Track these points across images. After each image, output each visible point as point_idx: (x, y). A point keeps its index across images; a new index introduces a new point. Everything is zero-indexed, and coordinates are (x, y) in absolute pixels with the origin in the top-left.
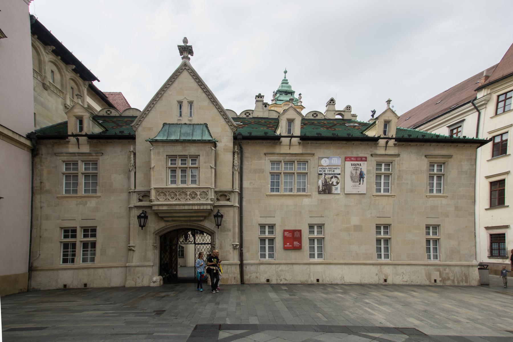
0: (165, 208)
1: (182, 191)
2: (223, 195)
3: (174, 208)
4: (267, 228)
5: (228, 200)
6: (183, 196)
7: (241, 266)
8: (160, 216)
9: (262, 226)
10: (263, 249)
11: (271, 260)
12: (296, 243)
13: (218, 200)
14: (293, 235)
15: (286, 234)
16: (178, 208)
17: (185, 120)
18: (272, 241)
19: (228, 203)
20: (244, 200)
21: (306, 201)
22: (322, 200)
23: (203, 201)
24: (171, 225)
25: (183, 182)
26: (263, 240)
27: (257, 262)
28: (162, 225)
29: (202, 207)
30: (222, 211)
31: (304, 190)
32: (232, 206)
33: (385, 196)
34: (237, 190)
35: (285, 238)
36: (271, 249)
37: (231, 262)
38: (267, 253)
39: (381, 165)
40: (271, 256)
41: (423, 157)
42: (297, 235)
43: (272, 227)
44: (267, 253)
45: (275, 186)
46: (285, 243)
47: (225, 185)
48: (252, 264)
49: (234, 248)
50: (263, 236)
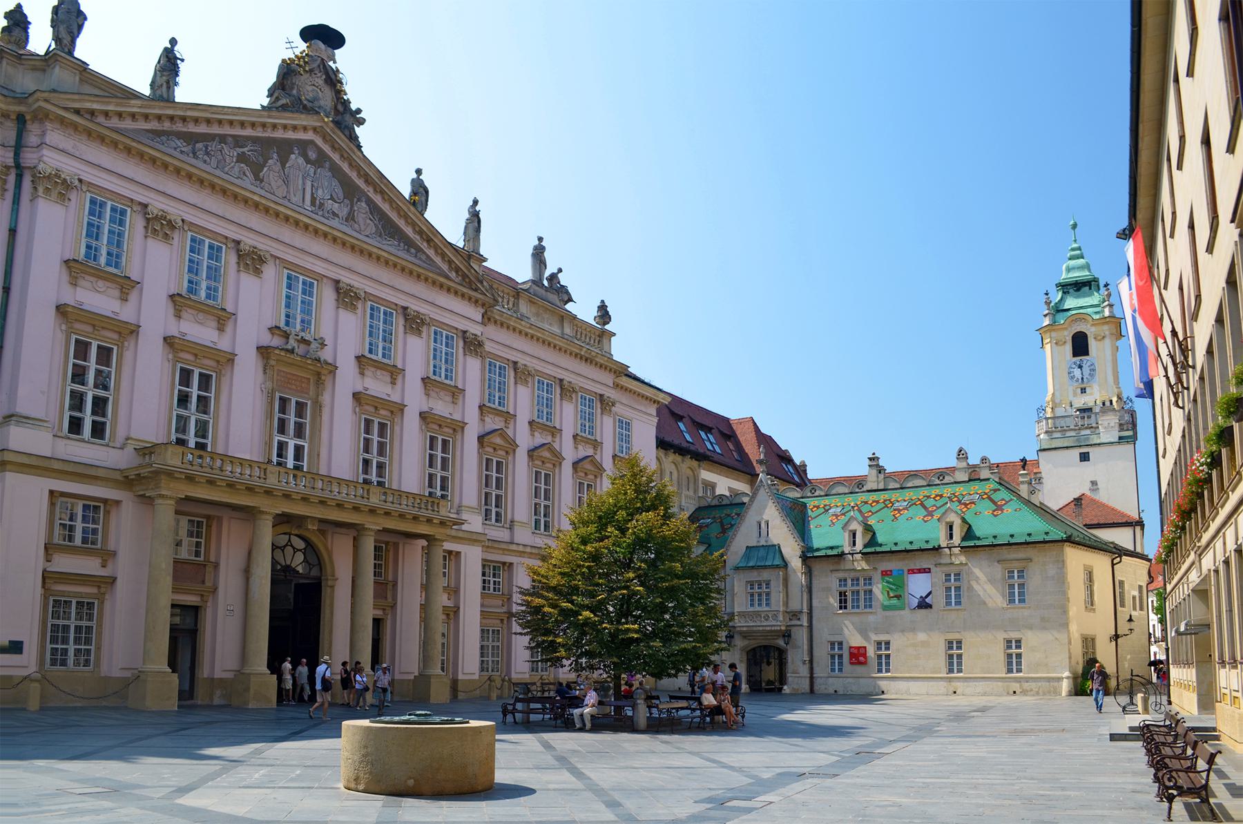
0: (745, 629)
1: (758, 614)
2: (795, 615)
3: (752, 629)
4: (836, 644)
5: (799, 619)
6: (759, 618)
7: (812, 678)
8: (745, 635)
9: (833, 644)
10: (833, 664)
11: (840, 674)
12: (861, 659)
13: (790, 620)
14: (859, 651)
15: (852, 650)
16: (755, 629)
17: (763, 543)
18: (840, 656)
19: (799, 623)
20: (814, 619)
21: (871, 618)
22: (886, 617)
23: (774, 623)
24: (754, 644)
25: (760, 605)
26: (833, 657)
27: (826, 675)
28: (746, 642)
29: (773, 628)
30: (794, 630)
31: (871, 606)
32: (801, 625)
33: (958, 610)
34: (805, 610)
35: (851, 653)
36: (841, 664)
37: (801, 675)
38: (837, 667)
39: (950, 575)
40: (841, 670)
41: (996, 564)
42: (862, 651)
43: (840, 643)
44: (837, 667)
45: (843, 604)
46: (851, 659)
47: (795, 605)
48: (821, 677)
49: (804, 662)
50: (832, 652)
